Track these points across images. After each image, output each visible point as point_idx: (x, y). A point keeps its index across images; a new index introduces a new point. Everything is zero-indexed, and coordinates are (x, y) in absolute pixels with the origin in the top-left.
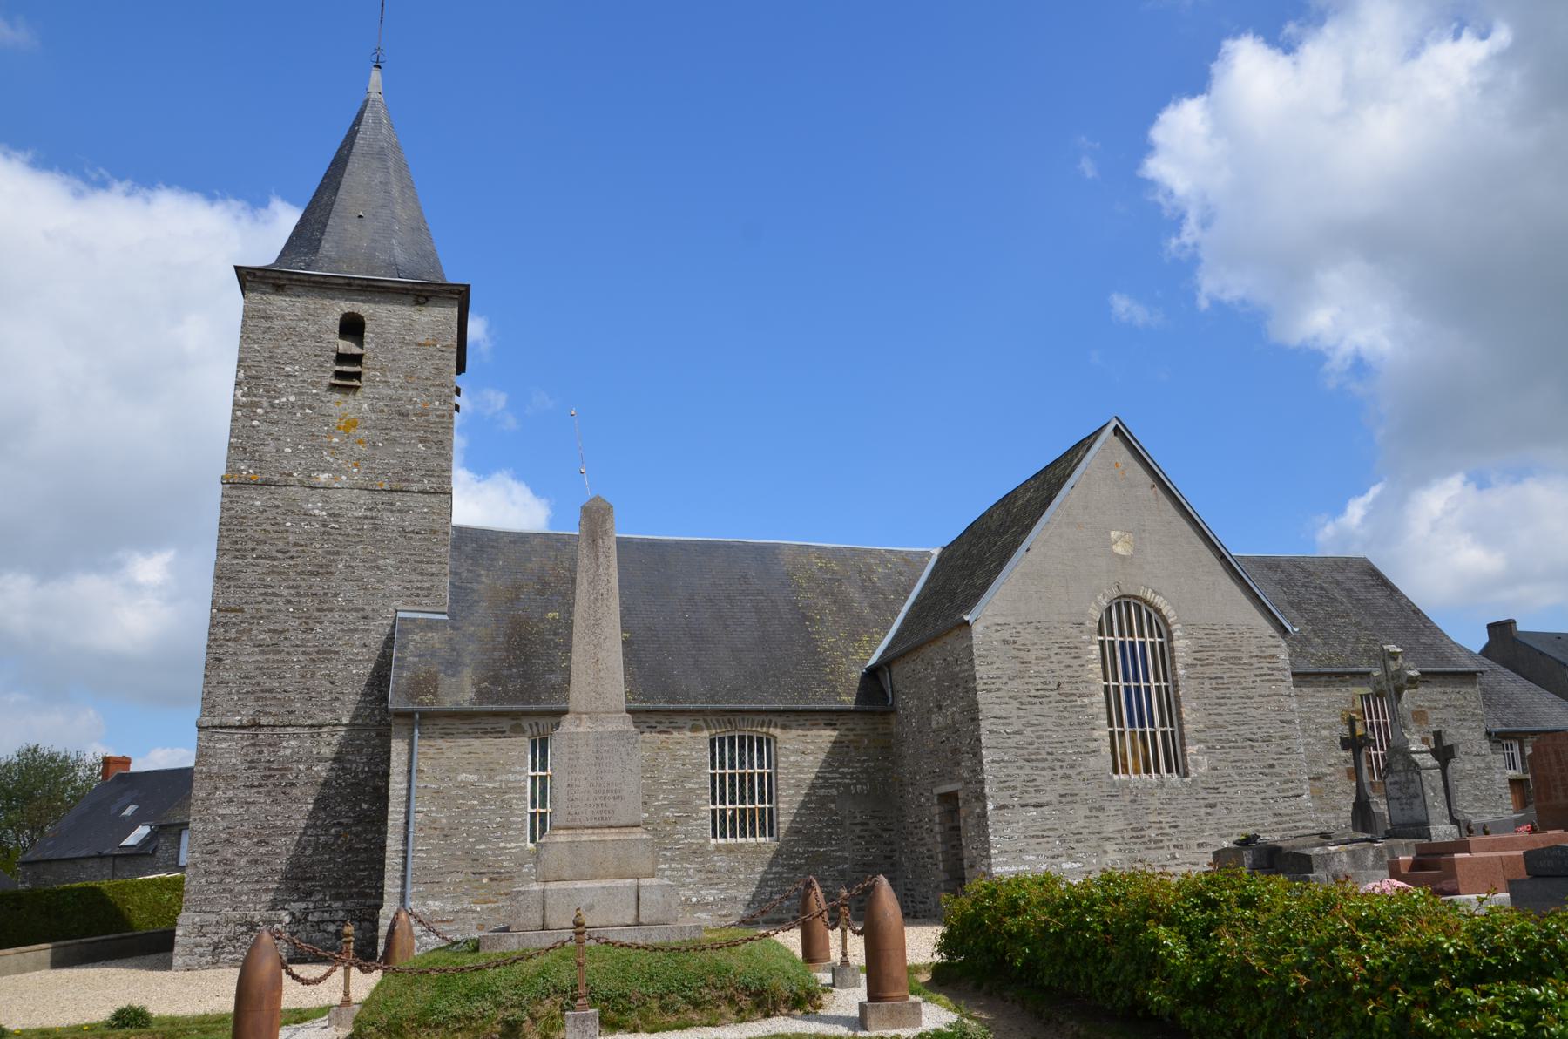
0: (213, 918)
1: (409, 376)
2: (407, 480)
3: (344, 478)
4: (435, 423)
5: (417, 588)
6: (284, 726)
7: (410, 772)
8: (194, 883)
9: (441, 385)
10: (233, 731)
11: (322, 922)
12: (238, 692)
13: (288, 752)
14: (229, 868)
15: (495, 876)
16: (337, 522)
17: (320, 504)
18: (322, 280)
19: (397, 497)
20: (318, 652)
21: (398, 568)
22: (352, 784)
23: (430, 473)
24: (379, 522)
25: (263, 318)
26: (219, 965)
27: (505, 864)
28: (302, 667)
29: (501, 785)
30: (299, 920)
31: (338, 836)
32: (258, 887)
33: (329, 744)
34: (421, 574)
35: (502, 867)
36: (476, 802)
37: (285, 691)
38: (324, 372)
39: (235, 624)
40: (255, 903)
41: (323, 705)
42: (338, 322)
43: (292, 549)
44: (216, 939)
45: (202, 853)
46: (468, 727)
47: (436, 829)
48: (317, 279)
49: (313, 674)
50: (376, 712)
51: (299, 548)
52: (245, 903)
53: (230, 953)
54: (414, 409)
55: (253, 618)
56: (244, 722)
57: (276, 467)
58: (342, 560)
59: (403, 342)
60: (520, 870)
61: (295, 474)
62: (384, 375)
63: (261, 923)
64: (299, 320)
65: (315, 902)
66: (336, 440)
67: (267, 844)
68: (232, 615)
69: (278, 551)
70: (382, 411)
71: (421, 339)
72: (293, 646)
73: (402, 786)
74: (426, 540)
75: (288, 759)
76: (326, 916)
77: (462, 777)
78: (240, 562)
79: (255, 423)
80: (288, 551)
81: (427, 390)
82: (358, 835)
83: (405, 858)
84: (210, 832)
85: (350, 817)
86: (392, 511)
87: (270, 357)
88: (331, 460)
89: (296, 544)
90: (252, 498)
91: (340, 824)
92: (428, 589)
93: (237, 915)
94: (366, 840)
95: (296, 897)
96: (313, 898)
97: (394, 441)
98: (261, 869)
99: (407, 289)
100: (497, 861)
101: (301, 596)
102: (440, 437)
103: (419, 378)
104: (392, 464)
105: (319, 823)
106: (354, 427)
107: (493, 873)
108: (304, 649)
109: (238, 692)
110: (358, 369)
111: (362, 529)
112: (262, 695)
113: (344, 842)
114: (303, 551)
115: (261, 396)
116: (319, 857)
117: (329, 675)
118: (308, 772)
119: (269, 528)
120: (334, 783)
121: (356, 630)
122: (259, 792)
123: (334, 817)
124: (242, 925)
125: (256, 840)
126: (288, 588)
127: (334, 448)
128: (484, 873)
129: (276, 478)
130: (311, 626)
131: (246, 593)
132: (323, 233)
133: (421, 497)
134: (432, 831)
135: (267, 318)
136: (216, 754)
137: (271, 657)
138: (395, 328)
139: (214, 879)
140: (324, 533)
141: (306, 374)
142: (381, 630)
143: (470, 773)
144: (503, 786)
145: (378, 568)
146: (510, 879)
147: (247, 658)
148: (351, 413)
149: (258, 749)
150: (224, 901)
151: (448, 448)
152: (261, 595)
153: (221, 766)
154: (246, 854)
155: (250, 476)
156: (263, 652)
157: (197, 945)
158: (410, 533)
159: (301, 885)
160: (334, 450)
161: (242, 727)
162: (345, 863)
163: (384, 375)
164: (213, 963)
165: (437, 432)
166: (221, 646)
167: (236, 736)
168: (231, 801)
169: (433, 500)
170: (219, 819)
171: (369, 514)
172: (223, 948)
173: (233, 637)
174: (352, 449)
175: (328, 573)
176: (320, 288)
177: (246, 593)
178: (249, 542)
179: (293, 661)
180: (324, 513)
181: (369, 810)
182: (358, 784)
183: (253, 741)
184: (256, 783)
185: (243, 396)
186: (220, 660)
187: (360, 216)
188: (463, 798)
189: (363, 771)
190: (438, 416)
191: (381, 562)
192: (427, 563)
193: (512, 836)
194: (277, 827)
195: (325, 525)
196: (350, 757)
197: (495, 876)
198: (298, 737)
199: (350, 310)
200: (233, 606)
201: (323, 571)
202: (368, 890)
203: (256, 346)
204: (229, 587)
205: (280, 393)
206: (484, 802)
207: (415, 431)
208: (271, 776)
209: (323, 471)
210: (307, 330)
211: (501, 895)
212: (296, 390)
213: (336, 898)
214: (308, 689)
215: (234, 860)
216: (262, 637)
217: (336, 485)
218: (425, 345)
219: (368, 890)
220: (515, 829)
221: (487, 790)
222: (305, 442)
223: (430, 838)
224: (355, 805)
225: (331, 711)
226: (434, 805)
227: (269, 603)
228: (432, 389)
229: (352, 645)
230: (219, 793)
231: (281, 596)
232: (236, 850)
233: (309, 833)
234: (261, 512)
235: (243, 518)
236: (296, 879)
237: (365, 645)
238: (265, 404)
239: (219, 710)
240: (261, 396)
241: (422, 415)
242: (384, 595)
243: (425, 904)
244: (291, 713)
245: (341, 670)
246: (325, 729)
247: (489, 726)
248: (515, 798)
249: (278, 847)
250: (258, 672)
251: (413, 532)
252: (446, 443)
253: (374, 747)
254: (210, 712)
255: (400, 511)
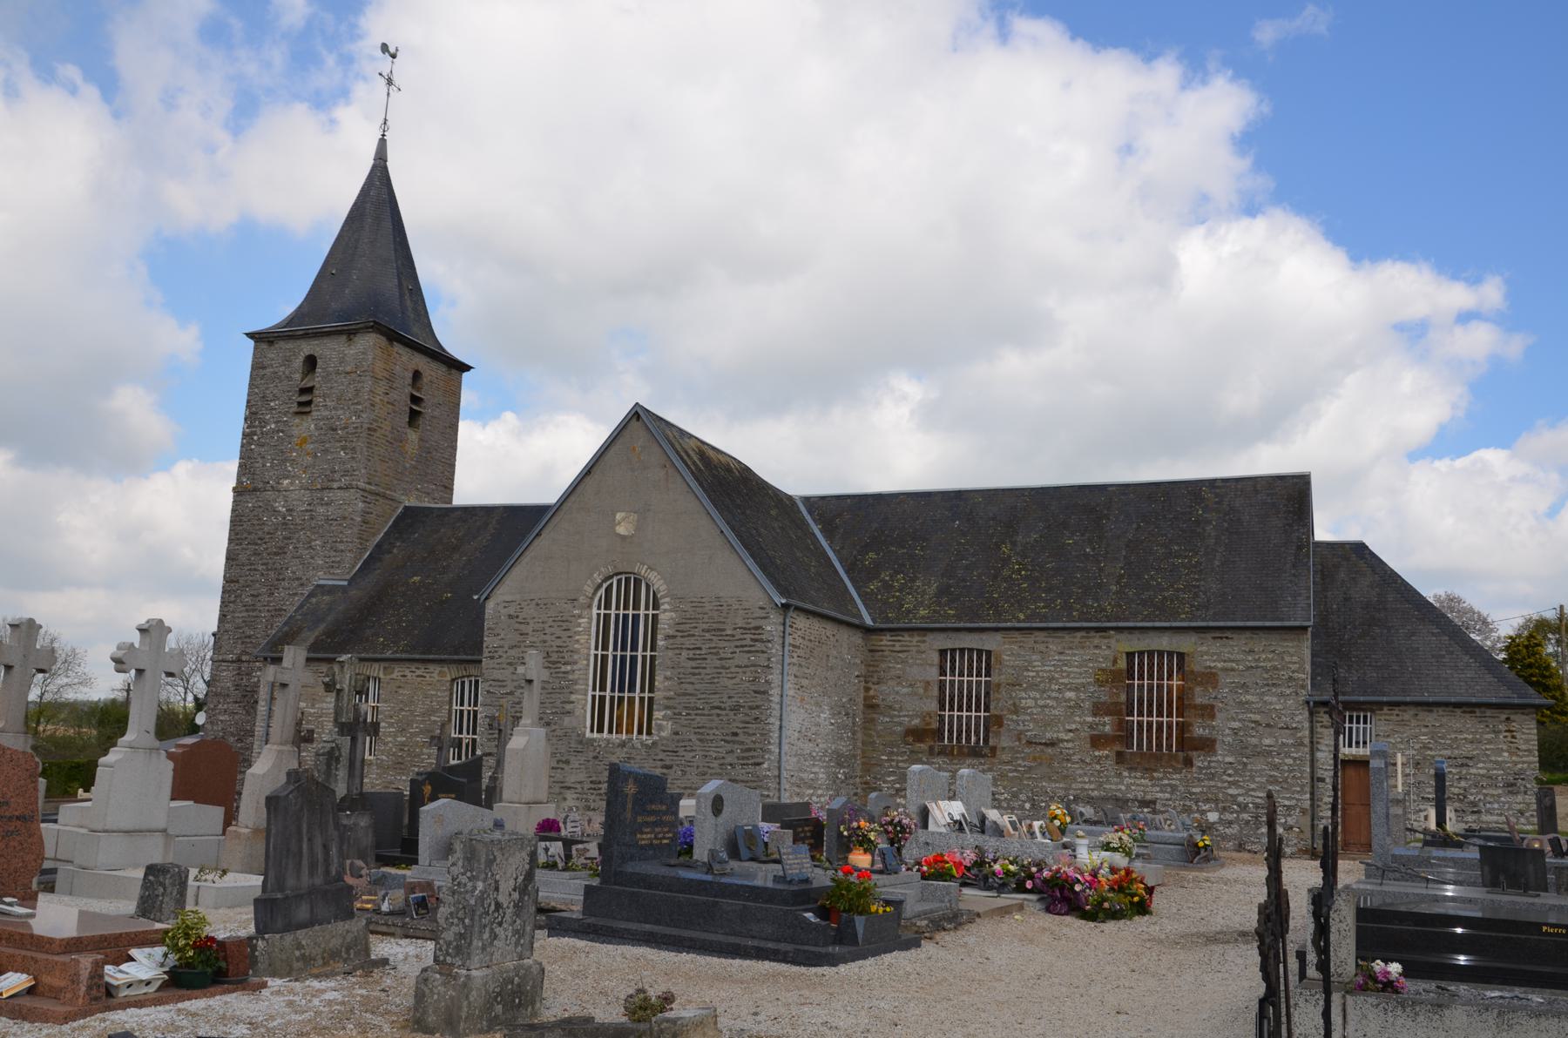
9: (357, 404)
49: (272, 625)
59: (338, 373)
71: (348, 369)
79: (253, 447)
89: (268, 533)
121: (296, 594)
133: (340, 493)
137: (251, 614)
156: (247, 611)
161: (232, 662)
201: (281, 552)
209: (286, 478)
228: (352, 407)
239: (223, 650)
255: (327, 504)
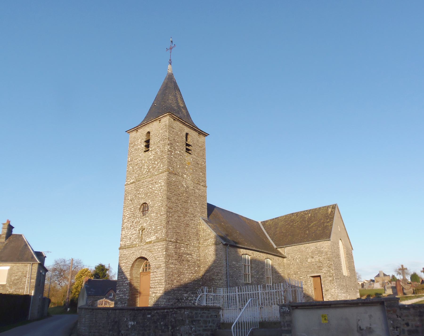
8: (166, 286)
49: (186, 230)
69: (178, 194)
79: (172, 157)
95: (185, 293)
124: (177, 300)
161: (174, 242)
173: (171, 216)
201: (186, 202)
245: (190, 230)
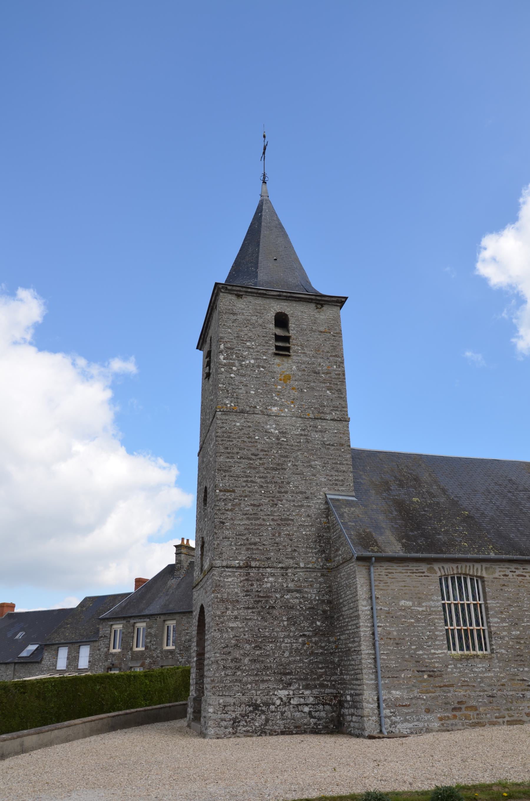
0: (231, 700)
1: (317, 350)
2: (322, 413)
3: (286, 410)
4: (335, 378)
5: (336, 480)
6: (265, 568)
7: (371, 598)
8: (217, 675)
9: (336, 356)
10: (235, 570)
11: (300, 705)
12: (236, 545)
13: (269, 585)
14: (238, 664)
15: (431, 673)
16: (285, 437)
17: (274, 426)
18: (265, 292)
19: (318, 422)
20: (281, 520)
21: (323, 467)
22: (310, 608)
23: (335, 408)
24: (310, 438)
25: (232, 314)
26: (238, 734)
27: (437, 665)
28: (272, 529)
29: (426, 609)
30: (285, 703)
31: (304, 644)
32: (257, 679)
33: (293, 580)
34: (337, 471)
35: (434, 667)
36: (413, 621)
37: (264, 545)
38: (269, 346)
39: (230, 500)
40: (256, 690)
41: (287, 554)
42: (274, 318)
43: (260, 454)
44: (234, 716)
45: (220, 653)
46: (402, 568)
47: (390, 639)
48: (262, 291)
49: (280, 533)
50: (319, 560)
51: (265, 453)
52: (250, 690)
53: (244, 726)
54: (322, 370)
55: (241, 496)
56: (241, 564)
57: (246, 402)
58: (290, 461)
59: (312, 330)
60: (446, 670)
61: (258, 407)
62: (303, 349)
63: (261, 705)
64: (252, 316)
65: (293, 691)
66: (279, 387)
67: (261, 648)
68: (228, 494)
69: (253, 454)
70: (304, 370)
71: (322, 329)
72: (266, 515)
73: (367, 608)
74: (338, 450)
75: (269, 590)
76: (302, 700)
77: (402, 603)
78: (231, 460)
79: (232, 375)
80: (258, 455)
81: (328, 358)
82: (316, 643)
83: (375, 659)
84: (225, 639)
85: (310, 631)
86: (316, 431)
87: (238, 337)
88: (278, 399)
89: (262, 450)
90: (234, 421)
91: (304, 635)
92: (342, 481)
93: (245, 699)
94: (322, 647)
95: (281, 687)
96: (292, 688)
97: (312, 389)
98: (258, 666)
99: (312, 299)
100: (431, 663)
101: (268, 483)
102: (339, 387)
103: (323, 351)
104: (313, 403)
105: (291, 634)
106: (289, 379)
107: (430, 671)
108: (273, 517)
109: (236, 545)
110: (288, 345)
111: (300, 442)
112: (250, 547)
113: (308, 648)
114: (267, 455)
115: (234, 360)
116: (293, 658)
117: (289, 535)
118: (282, 599)
119: (246, 439)
120: (298, 607)
121: (302, 506)
122: (253, 612)
123: (300, 631)
124: (250, 706)
125: (253, 645)
126: (260, 478)
127: (279, 392)
128: (424, 671)
129: (248, 409)
130: (276, 502)
131: (235, 480)
132: (257, 268)
133: (332, 423)
134: (389, 641)
135: (234, 314)
136: (225, 585)
137: (253, 522)
138: (306, 322)
139: (229, 672)
140: (278, 444)
141: (259, 347)
142: (317, 506)
143: (406, 600)
144: (428, 610)
145: (312, 467)
146: (441, 676)
147: (239, 522)
148: (286, 371)
149: (250, 583)
150: (236, 688)
151: (344, 394)
152: (245, 481)
153: (228, 594)
154: (248, 655)
155: (232, 407)
156: (248, 519)
157: (222, 720)
158: (328, 445)
159: (284, 678)
160: (279, 393)
161: (240, 567)
162: (310, 663)
163: (303, 349)
164: (233, 734)
165: (337, 384)
166: (223, 514)
167: (236, 574)
168: (236, 617)
169: (340, 425)
170: (230, 630)
171: (303, 433)
172: (239, 722)
173: (230, 508)
174: (289, 392)
175: (282, 469)
176: (263, 297)
177: (235, 480)
178: (235, 448)
179: (267, 525)
180: (277, 431)
181: (321, 626)
182: (313, 608)
183: (247, 577)
184: (251, 606)
185: (224, 359)
186: (223, 523)
187: (276, 260)
188: (405, 617)
189: (315, 599)
190: (336, 374)
191: (313, 463)
192: (340, 464)
193: (437, 645)
194: (266, 636)
195: (278, 439)
196: (306, 590)
197: (431, 673)
198: (274, 575)
199: (280, 311)
200: (228, 488)
201: (279, 467)
202: (325, 683)
203: (229, 330)
204: (225, 476)
205: (245, 358)
206: (418, 620)
207: (324, 383)
208: (259, 601)
209: (274, 406)
210: (257, 322)
211: (436, 687)
212: (254, 357)
213: (307, 687)
214: (277, 544)
215: (241, 659)
216: (247, 509)
217: (282, 414)
218: (324, 332)
219: (325, 683)
220: (439, 640)
221: (419, 612)
222: (262, 388)
223: (388, 645)
224: (312, 623)
225: (293, 558)
226: (388, 622)
227: (249, 487)
228: (331, 358)
229: (301, 515)
230: (229, 612)
231: (256, 483)
232: (242, 652)
233: (286, 641)
234: (241, 430)
235: (231, 433)
236: (280, 674)
237: (308, 516)
238: (237, 364)
239: (225, 556)
240: (234, 360)
241: (327, 373)
242: (317, 484)
243: (390, 693)
244: (268, 559)
245: (296, 532)
246: (290, 571)
247: (414, 568)
248: (436, 618)
249: (268, 651)
250: (246, 532)
251: (329, 445)
252: (343, 390)
253: (320, 583)
254: (219, 557)
255: (321, 431)
